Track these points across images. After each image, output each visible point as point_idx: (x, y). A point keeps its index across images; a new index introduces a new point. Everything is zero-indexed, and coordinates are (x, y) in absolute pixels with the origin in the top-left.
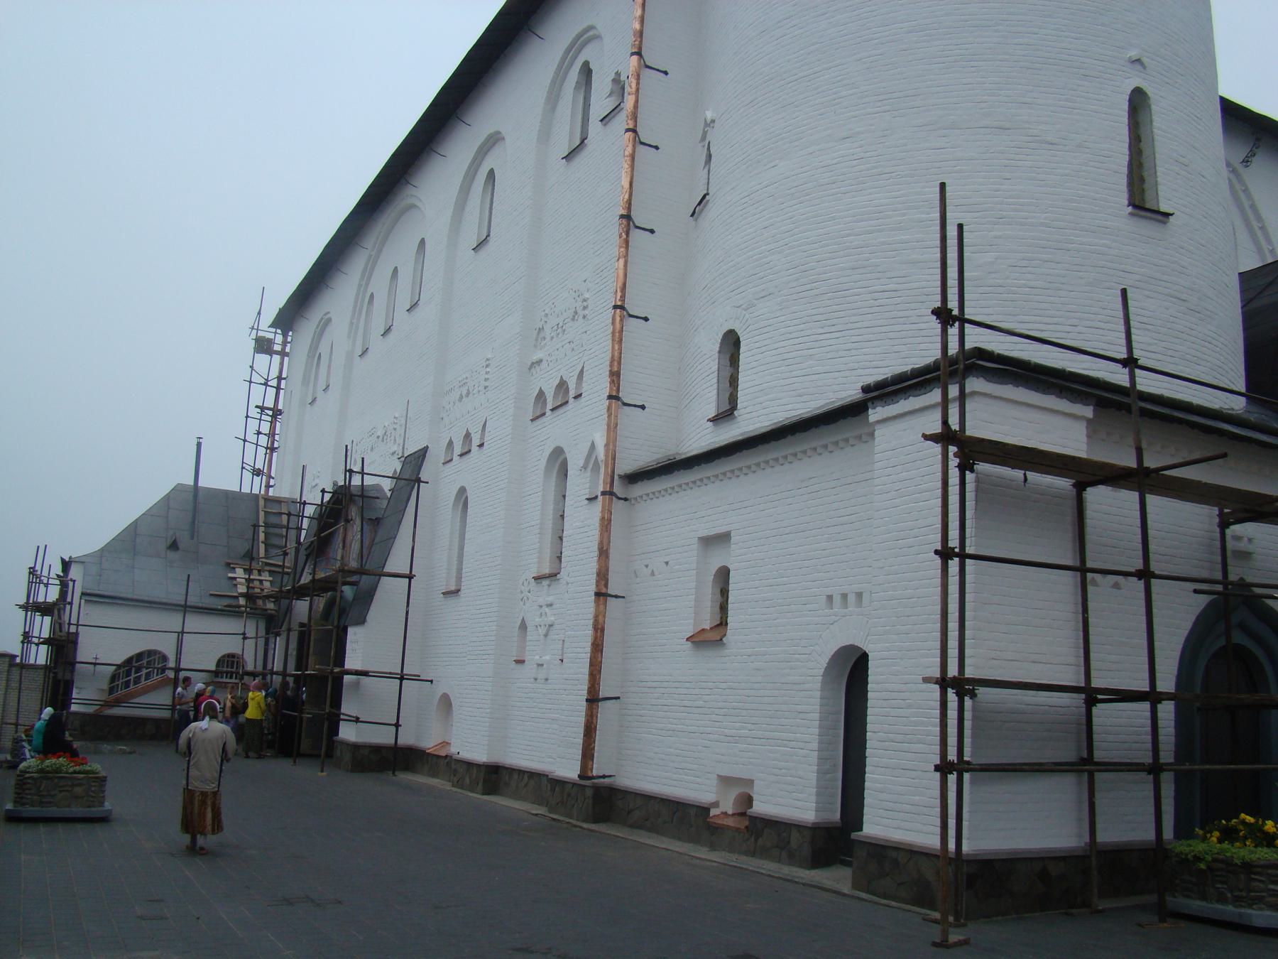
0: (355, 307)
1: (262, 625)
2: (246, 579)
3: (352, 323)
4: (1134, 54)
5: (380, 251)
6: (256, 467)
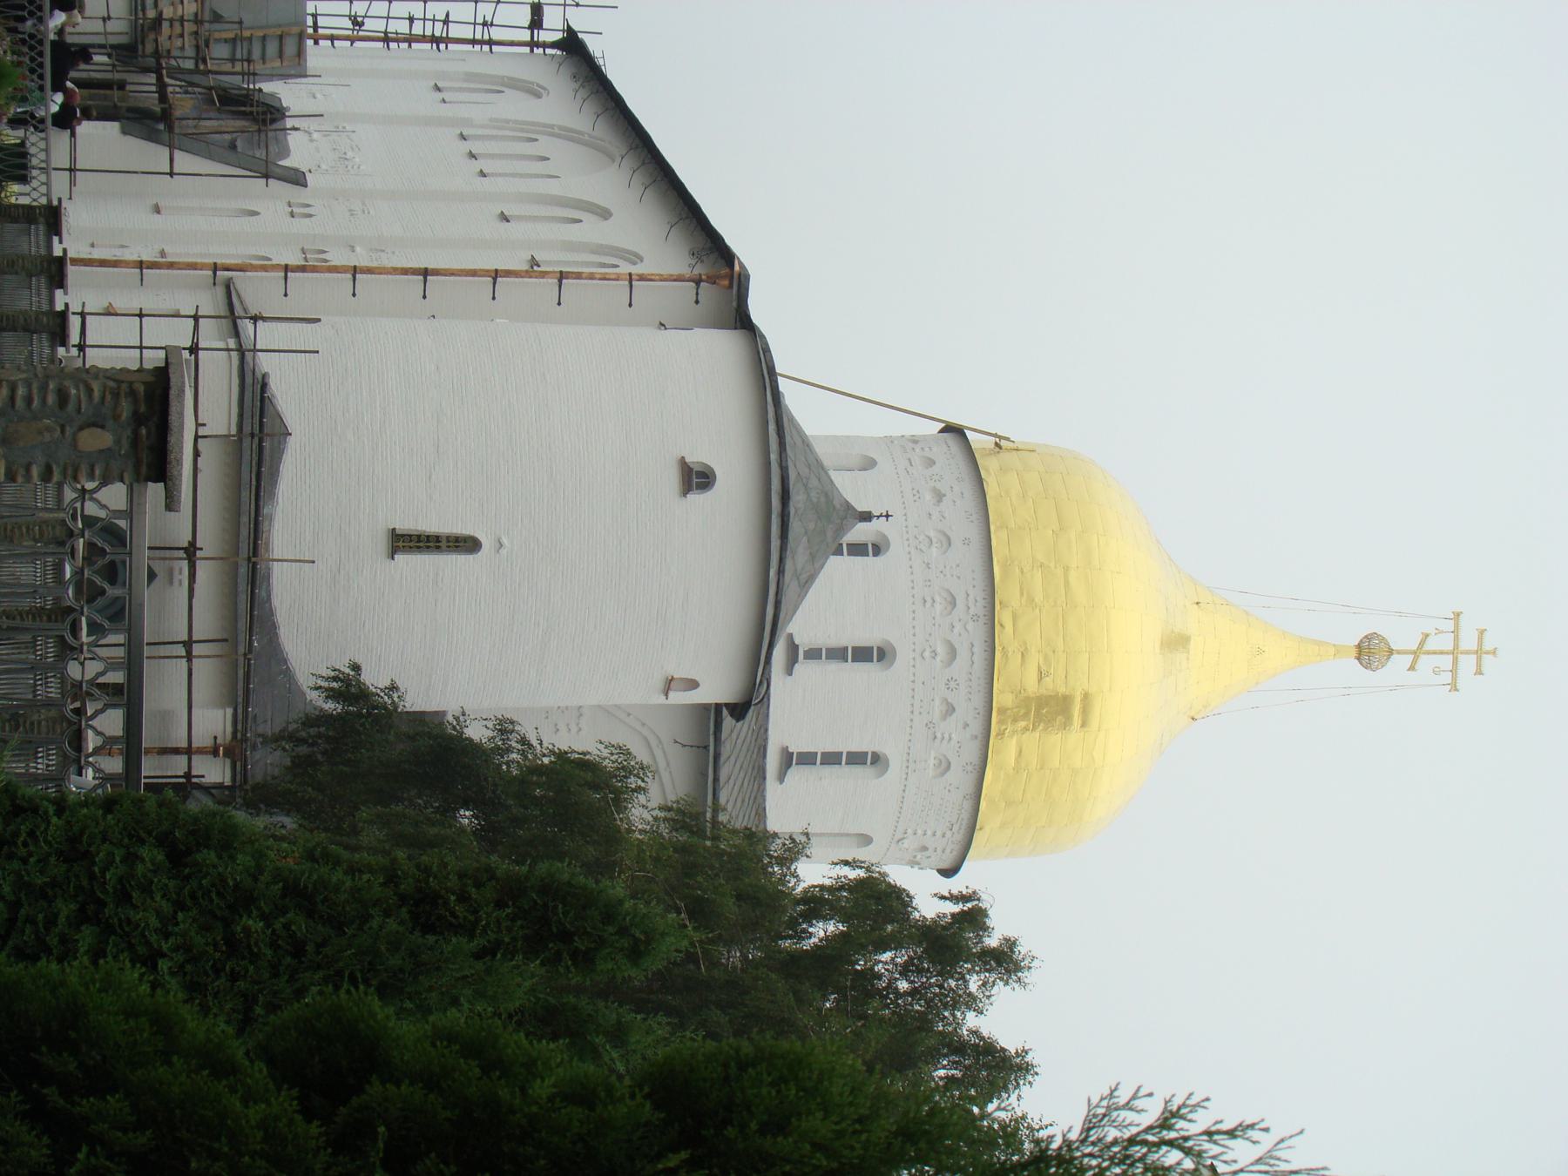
0: (533, 124)
1: (124, 40)
2: (182, 17)
3: (507, 121)
4: (505, 541)
5: (586, 144)
6: (366, 20)
